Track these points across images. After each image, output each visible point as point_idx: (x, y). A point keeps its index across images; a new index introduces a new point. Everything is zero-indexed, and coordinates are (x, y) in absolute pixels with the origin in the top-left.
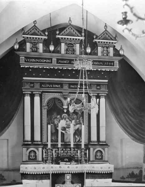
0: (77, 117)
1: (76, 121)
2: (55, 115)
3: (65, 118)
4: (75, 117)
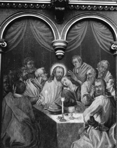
0: (97, 72)
1: (94, 84)
3: (58, 74)
4: (89, 71)
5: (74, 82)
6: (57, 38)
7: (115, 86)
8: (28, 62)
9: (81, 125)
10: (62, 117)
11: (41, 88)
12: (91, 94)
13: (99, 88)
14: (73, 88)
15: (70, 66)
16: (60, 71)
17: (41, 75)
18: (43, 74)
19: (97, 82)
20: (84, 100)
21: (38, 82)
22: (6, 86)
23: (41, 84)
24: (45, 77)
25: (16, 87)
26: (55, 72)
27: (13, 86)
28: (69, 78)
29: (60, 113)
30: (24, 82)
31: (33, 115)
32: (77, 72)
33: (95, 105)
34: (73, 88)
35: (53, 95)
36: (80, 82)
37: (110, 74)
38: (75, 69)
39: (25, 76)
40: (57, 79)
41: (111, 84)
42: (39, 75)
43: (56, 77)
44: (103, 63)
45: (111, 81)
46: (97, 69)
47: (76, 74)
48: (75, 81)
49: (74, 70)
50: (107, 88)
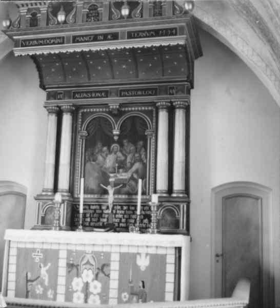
0: (136, 148)
1: (134, 155)
2: (99, 146)
4: (132, 148)
5: (123, 155)
6: (115, 129)
12: (133, 162)
14: (123, 158)
15: (122, 145)
20: (128, 165)
21: (104, 155)
29: (115, 173)
33: (134, 168)
34: (123, 158)
35: (112, 162)
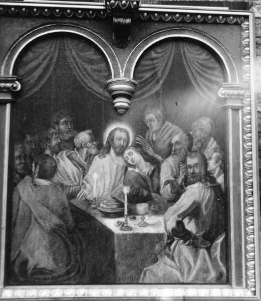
2: (62, 127)
6: (117, 74)
7: (223, 165)
8: (61, 119)
9: (159, 236)
10: (124, 223)
11: (86, 168)
12: (180, 181)
13: (194, 170)
14: (146, 168)
16: (121, 138)
17: (86, 144)
18: (90, 142)
19: (191, 158)
20: (166, 190)
21: (81, 157)
22: (20, 164)
23: (86, 160)
24: (94, 148)
25: (38, 167)
26: (112, 139)
27: (33, 165)
28: (138, 149)
29: (120, 214)
30: (54, 157)
31: (70, 219)
32: (154, 139)
33: (186, 201)
34: (146, 168)
35: (108, 181)
36: (159, 158)
37: (215, 143)
38: (149, 133)
39: (56, 147)
40: (115, 152)
41: (217, 162)
42: (81, 144)
43: (115, 148)
44: (201, 123)
45: (216, 157)
46: (191, 133)
47: (151, 143)
48: (150, 156)
49: (147, 135)
50: (208, 170)
